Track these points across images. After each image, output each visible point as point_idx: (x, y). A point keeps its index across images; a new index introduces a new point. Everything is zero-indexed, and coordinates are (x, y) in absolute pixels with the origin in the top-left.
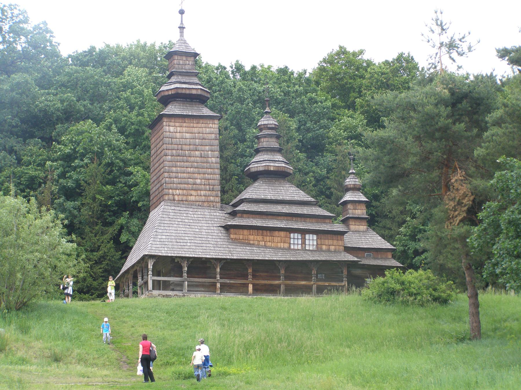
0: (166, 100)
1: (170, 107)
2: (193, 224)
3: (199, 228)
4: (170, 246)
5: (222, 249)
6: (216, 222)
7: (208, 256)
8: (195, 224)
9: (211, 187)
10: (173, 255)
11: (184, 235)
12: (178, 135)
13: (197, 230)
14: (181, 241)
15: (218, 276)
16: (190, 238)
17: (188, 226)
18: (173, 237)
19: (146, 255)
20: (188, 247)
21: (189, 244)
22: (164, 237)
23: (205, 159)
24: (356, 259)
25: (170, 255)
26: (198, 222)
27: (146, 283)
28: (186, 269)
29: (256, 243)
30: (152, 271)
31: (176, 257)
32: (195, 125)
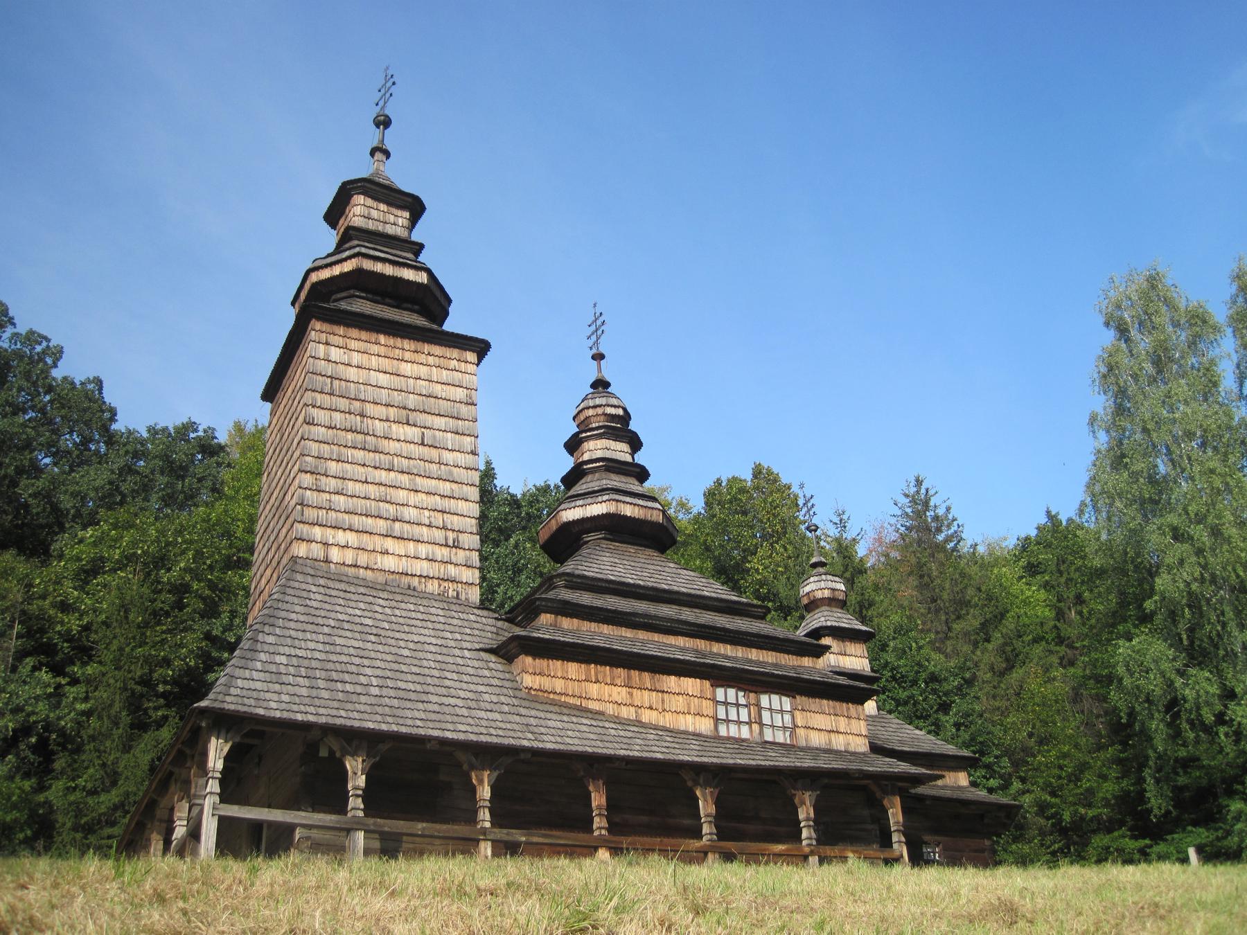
2: (390, 633)
3: (411, 645)
4: (304, 692)
5: (497, 716)
6: (468, 638)
7: (449, 735)
8: (397, 635)
9: (451, 535)
10: (311, 718)
11: (357, 661)
12: (352, 373)
13: (406, 652)
14: (347, 677)
16: (379, 672)
17: (373, 638)
18: (314, 664)
20: (373, 700)
21: (375, 691)
23: (434, 454)
26: (406, 629)
27: (194, 834)
28: (361, 781)
29: (610, 709)
30: (222, 782)
32: (408, 356)
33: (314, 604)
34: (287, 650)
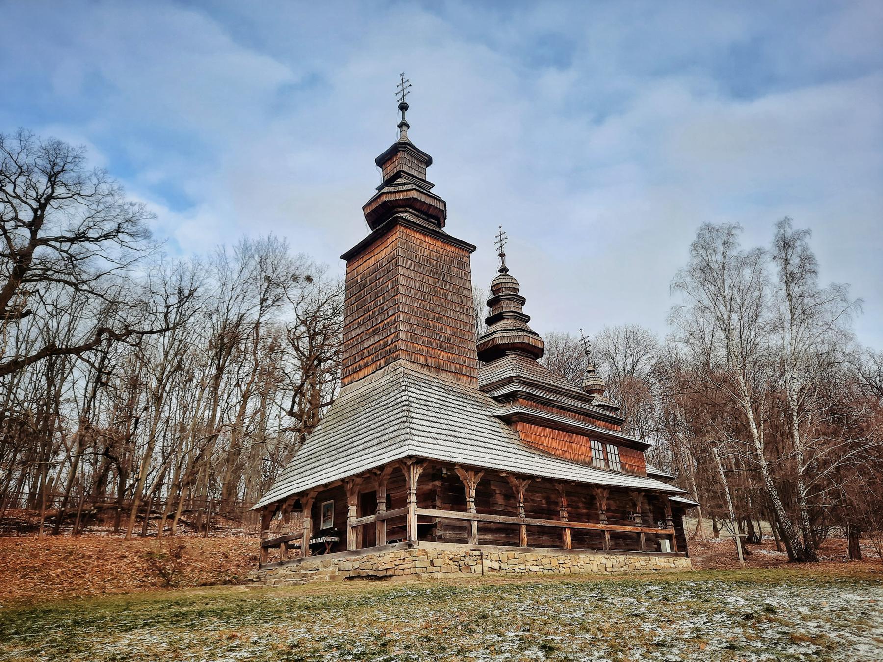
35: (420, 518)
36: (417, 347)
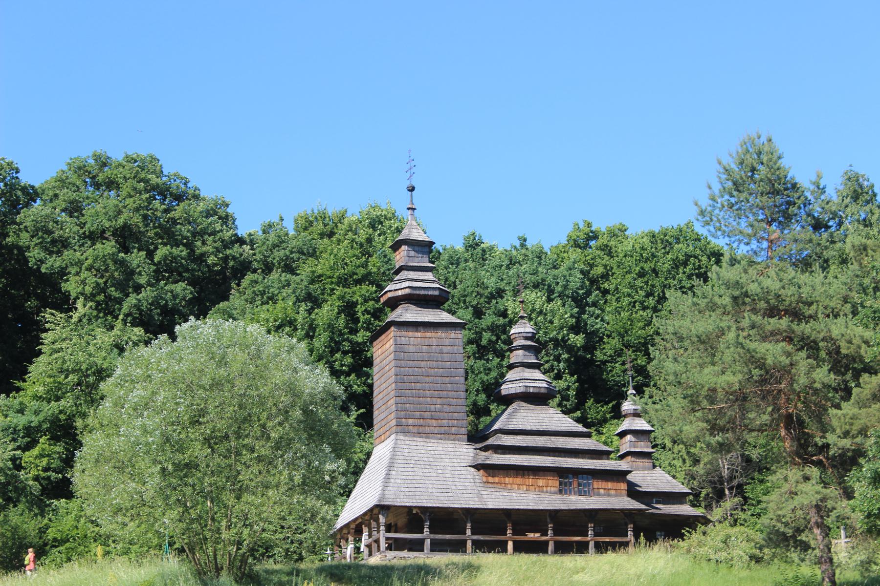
0: (394, 303)
1: (399, 310)
15: (468, 531)
19: (376, 506)
22: (399, 481)
24: (643, 507)
25: (407, 504)
31: (415, 507)
33: (406, 454)
34: (400, 477)
35: (387, 539)
36: (410, 421)
